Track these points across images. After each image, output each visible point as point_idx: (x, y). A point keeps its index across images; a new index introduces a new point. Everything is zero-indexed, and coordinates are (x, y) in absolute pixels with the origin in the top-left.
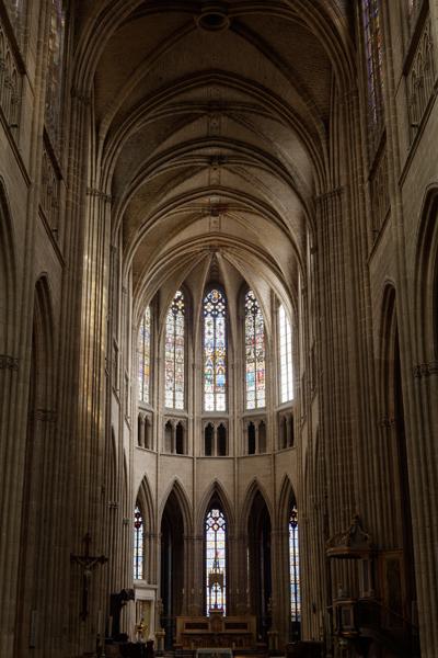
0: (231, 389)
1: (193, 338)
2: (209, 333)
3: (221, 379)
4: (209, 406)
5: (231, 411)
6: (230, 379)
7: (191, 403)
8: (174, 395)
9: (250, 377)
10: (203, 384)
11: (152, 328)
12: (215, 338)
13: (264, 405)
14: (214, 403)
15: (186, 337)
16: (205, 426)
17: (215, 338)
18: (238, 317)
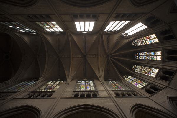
0: (155, 49)
1: (142, 63)
2: (142, 58)
3: (152, 53)
4: (159, 58)
5: (161, 49)
6: (151, 50)
7: (157, 66)
8: (153, 73)
9: (150, 43)
10: (154, 60)
11: (135, 77)
12: (143, 56)
13: (154, 35)
14: (158, 56)
15: (142, 66)
16: (167, 61)
17: (143, 56)
18: (138, 48)
